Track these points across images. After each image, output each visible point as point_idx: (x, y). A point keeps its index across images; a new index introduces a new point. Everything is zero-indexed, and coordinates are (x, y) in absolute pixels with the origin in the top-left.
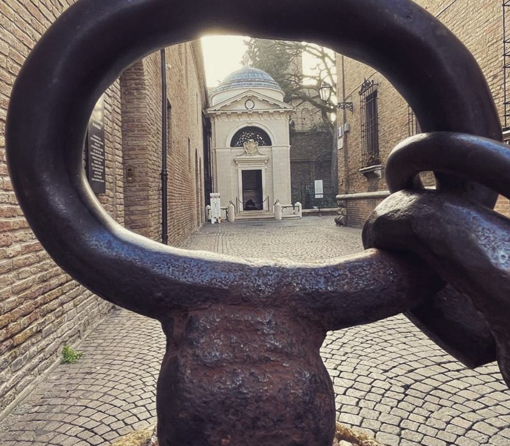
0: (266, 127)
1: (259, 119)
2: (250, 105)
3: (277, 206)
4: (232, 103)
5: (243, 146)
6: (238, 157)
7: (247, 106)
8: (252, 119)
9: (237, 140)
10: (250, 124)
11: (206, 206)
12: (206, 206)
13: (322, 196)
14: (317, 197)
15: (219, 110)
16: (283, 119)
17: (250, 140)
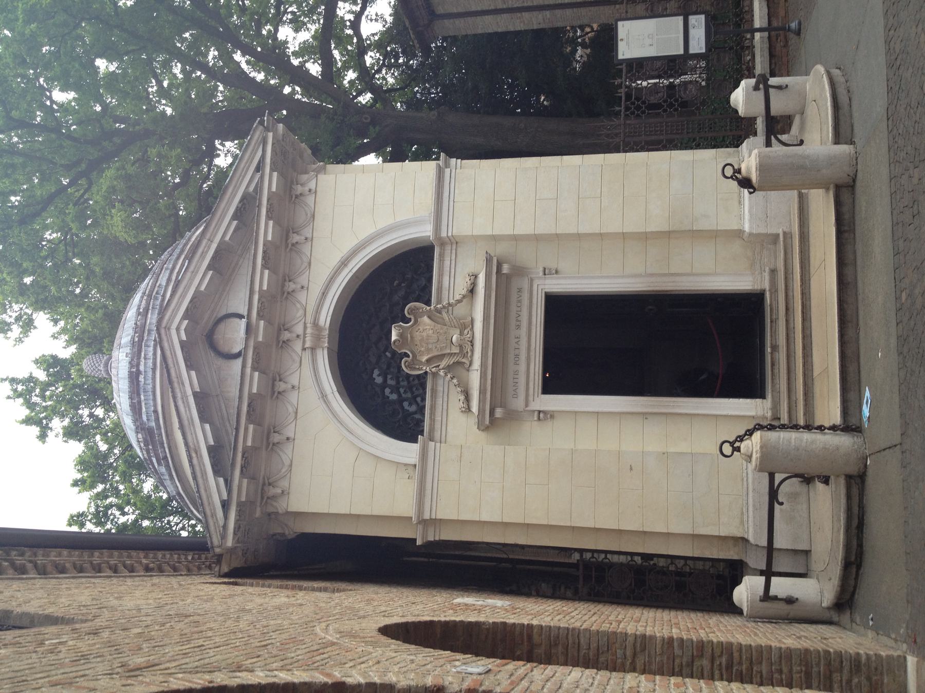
1: (302, 296)
2: (235, 335)
3: (763, 168)
4: (203, 419)
5: (421, 380)
6: (475, 408)
7: (236, 350)
8: (299, 329)
9: (389, 399)
10: (317, 338)
11: (736, 611)
12: (736, 611)
13: (698, 24)
14: (698, 44)
15: (229, 492)
16: (312, 185)
17: (394, 337)
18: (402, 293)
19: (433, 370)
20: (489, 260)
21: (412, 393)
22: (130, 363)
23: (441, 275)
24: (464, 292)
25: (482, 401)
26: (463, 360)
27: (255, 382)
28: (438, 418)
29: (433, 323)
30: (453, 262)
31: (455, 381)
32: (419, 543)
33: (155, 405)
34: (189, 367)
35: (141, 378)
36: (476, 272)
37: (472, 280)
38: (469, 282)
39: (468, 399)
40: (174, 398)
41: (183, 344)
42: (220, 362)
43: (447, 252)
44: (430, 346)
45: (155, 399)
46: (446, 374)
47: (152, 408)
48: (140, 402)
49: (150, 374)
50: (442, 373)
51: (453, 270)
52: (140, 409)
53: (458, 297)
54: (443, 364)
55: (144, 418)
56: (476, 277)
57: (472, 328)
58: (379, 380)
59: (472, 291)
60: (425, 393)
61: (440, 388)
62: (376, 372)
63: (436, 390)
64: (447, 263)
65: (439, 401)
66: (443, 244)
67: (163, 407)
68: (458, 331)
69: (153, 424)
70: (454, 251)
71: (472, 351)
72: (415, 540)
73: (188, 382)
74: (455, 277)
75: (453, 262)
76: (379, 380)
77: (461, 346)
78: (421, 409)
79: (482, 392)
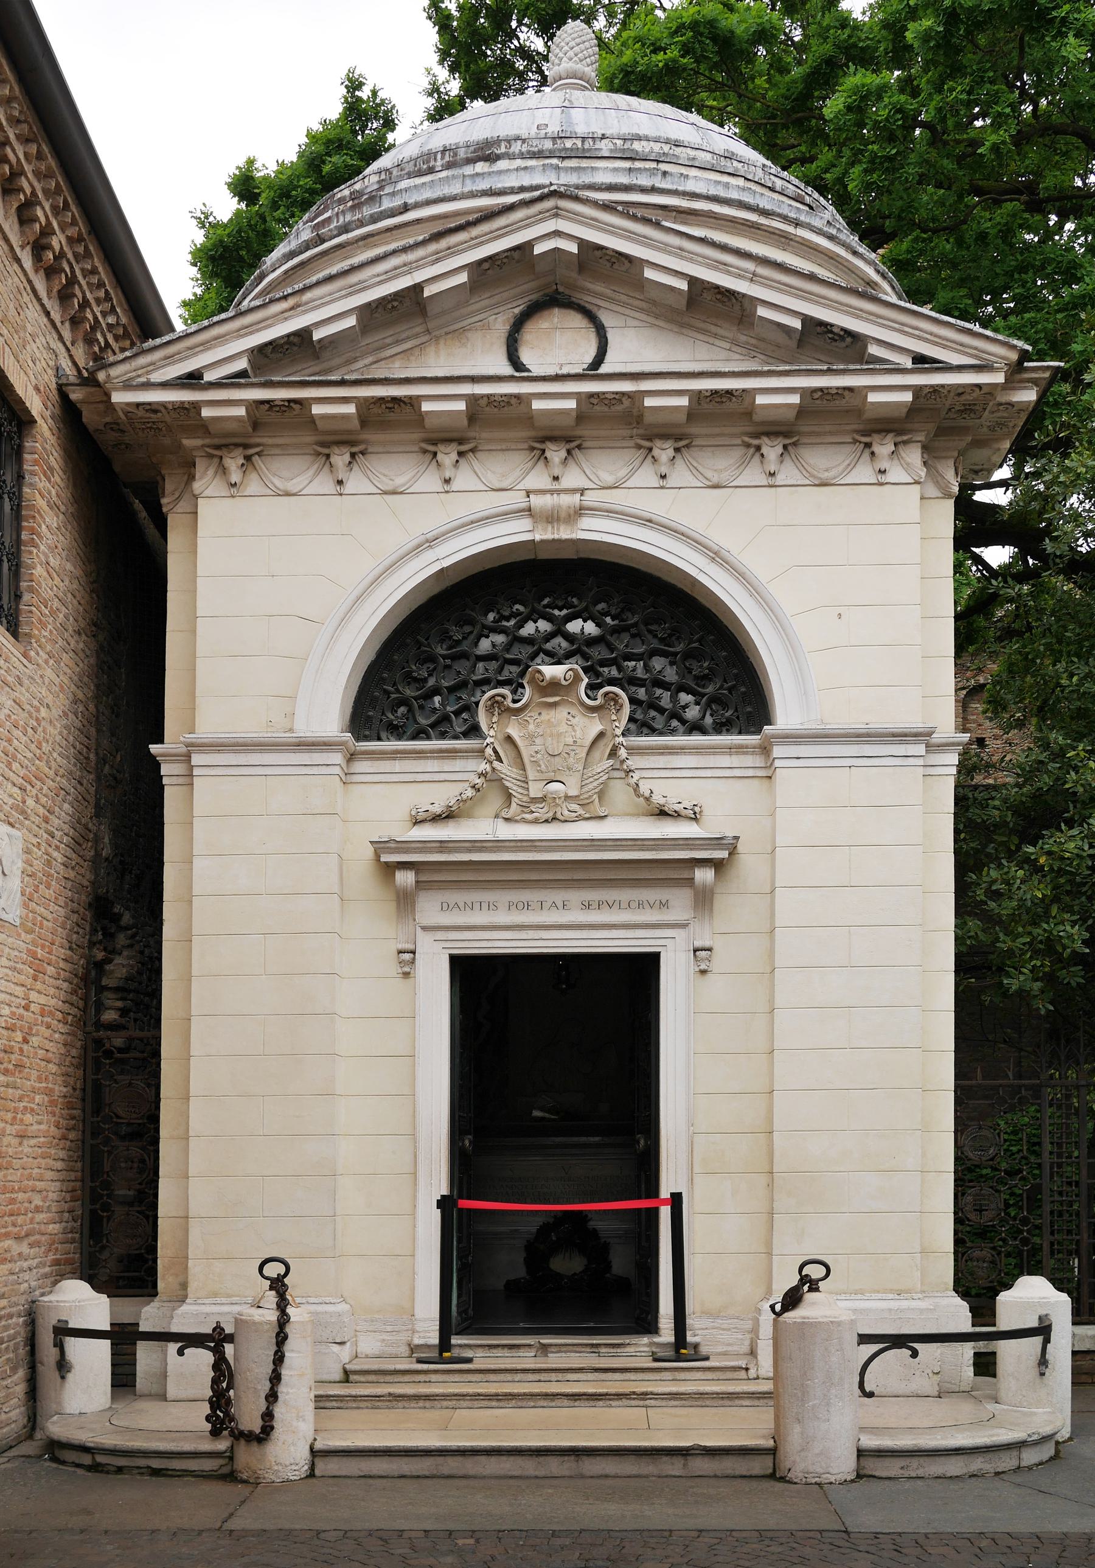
0: (716, 556)
7: (526, 356)
18: (671, 675)
19: (489, 751)
20: (717, 842)
21: (457, 713)
22: (517, 138)
23: (698, 750)
24: (657, 799)
25: (424, 846)
26: (514, 805)
27: (444, 405)
28: (397, 765)
29: (588, 743)
30: (728, 773)
31: (470, 793)
32: (154, 748)
33: (417, 205)
34: (478, 268)
35: (480, 167)
36: (704, 819)
37: (684, 812)
38: (677, 807)
39: (436, 819)
40: (405, 250)
41: (525, 248)
42: (501, 325)
43: (749, 760)
44: (538, 741)
45: (429, 202)
46: (481, 775)
47: (411, 201)
48: (431, 171)
49: (483, 185)
50: (484, 766)
51: (709, 773)
52: (420, 174)
53: (644, 788)
54: (506, 769)
55: (403, 184)
56: (696, 819)
57: (581, 818)
58: (485, 645)
59: (662, 813)
60: (456, 737)
61: (458, 764)
62: (500, 639)
63: (454, 758)
64: (725, 761)
65: (432, 765)
66: (765, 750)
67: (418, 221)
68: (573, 792)
69: (387, 204)
70: (750, 772)
71: (536, 821)
72: (160, 740)
73: (443, 271)
74: (697, 780)
75: (728, 773)
76: (485, 645)
77: (543, 799)
78: (420, 734)
79: (443, 846)
